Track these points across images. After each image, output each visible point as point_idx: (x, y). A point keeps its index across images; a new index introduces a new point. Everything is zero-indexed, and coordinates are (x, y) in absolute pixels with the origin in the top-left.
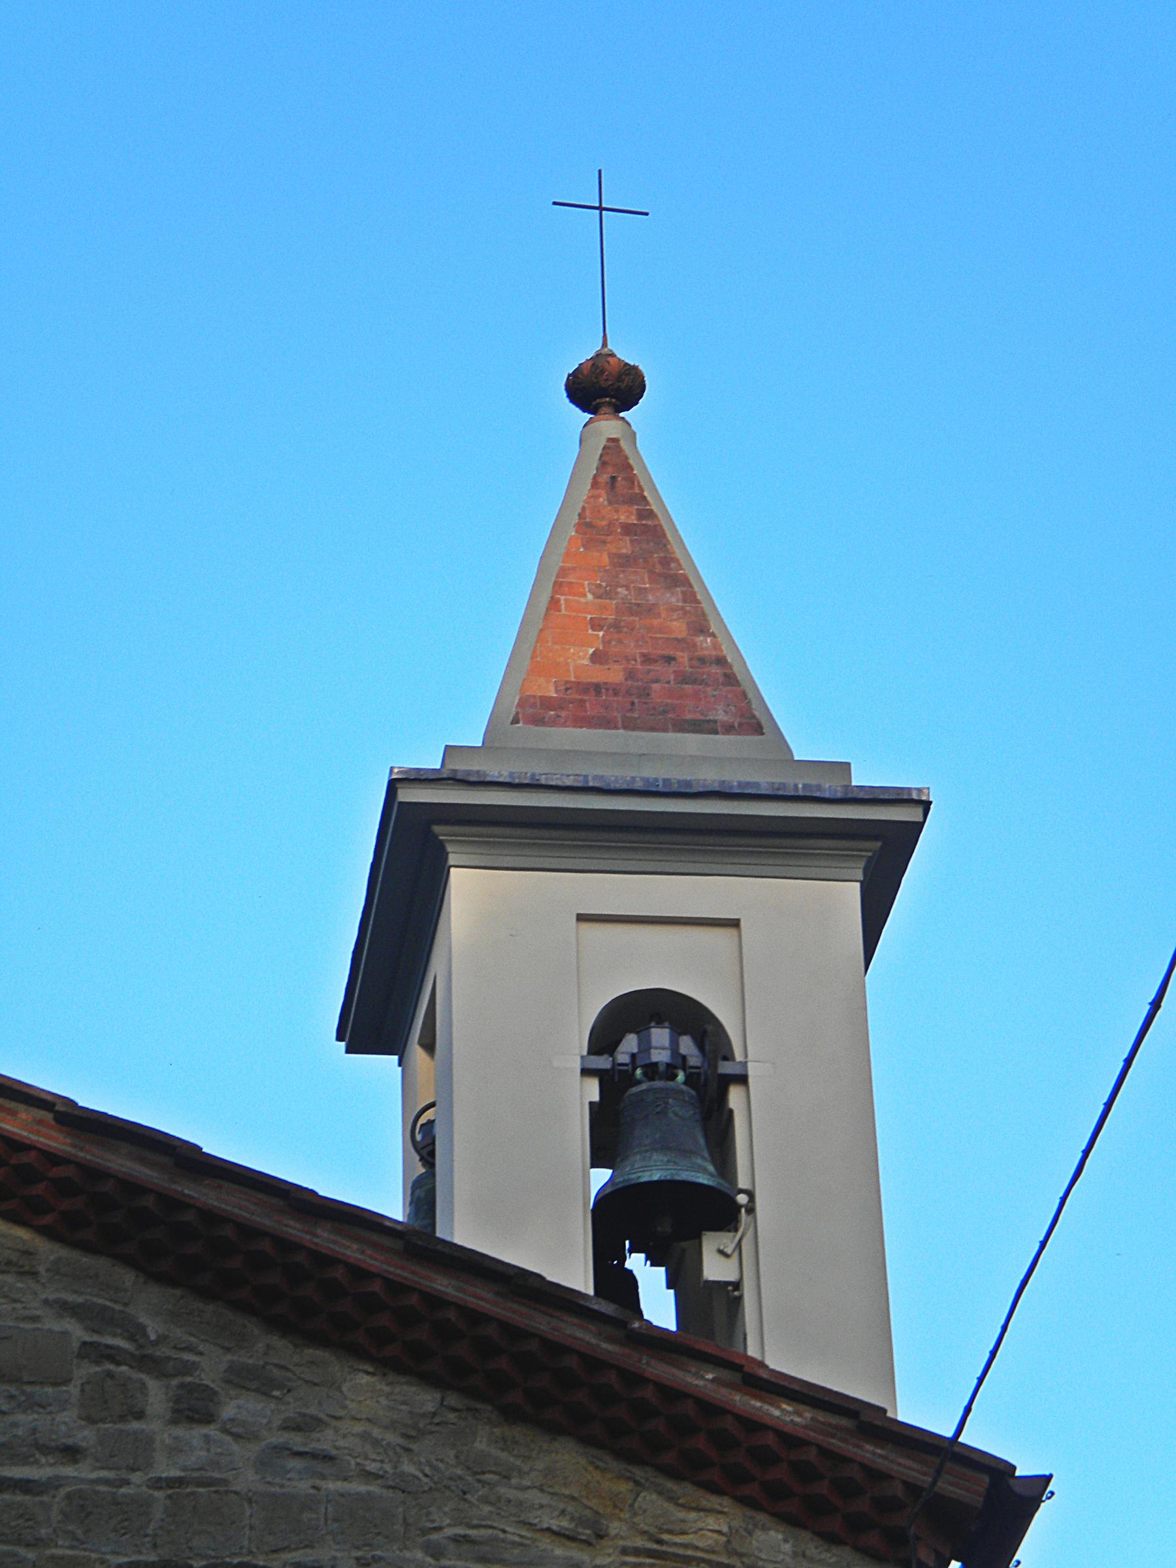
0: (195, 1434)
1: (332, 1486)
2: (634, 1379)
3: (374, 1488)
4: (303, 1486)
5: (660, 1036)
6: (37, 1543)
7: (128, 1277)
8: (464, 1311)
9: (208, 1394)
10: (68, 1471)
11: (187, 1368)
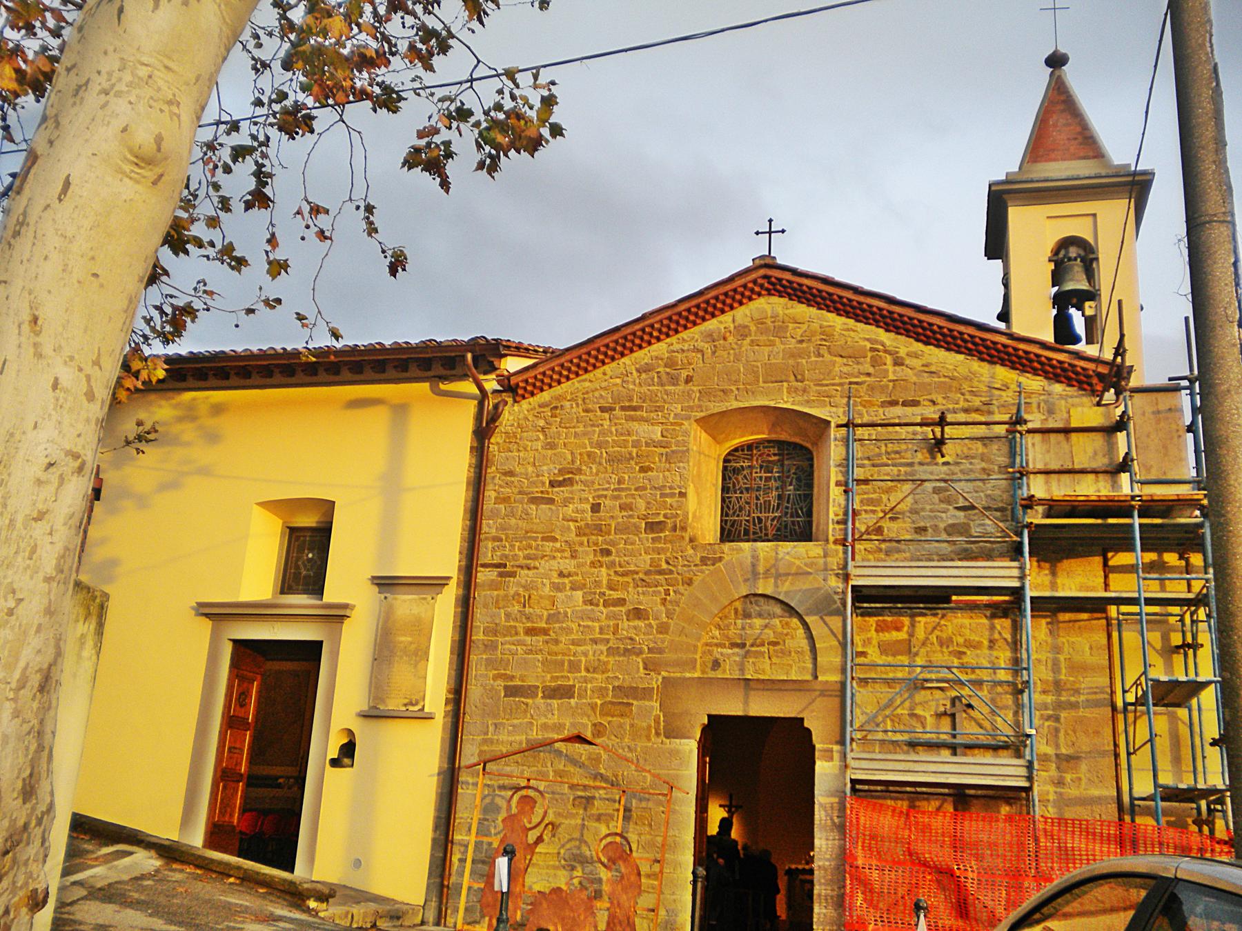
1: (937, 379)
2: (1016, 349)
4: (928, 380)
6: (860, 397)
9: (902, 358)
10: (868, 379)
11: (897, 352)
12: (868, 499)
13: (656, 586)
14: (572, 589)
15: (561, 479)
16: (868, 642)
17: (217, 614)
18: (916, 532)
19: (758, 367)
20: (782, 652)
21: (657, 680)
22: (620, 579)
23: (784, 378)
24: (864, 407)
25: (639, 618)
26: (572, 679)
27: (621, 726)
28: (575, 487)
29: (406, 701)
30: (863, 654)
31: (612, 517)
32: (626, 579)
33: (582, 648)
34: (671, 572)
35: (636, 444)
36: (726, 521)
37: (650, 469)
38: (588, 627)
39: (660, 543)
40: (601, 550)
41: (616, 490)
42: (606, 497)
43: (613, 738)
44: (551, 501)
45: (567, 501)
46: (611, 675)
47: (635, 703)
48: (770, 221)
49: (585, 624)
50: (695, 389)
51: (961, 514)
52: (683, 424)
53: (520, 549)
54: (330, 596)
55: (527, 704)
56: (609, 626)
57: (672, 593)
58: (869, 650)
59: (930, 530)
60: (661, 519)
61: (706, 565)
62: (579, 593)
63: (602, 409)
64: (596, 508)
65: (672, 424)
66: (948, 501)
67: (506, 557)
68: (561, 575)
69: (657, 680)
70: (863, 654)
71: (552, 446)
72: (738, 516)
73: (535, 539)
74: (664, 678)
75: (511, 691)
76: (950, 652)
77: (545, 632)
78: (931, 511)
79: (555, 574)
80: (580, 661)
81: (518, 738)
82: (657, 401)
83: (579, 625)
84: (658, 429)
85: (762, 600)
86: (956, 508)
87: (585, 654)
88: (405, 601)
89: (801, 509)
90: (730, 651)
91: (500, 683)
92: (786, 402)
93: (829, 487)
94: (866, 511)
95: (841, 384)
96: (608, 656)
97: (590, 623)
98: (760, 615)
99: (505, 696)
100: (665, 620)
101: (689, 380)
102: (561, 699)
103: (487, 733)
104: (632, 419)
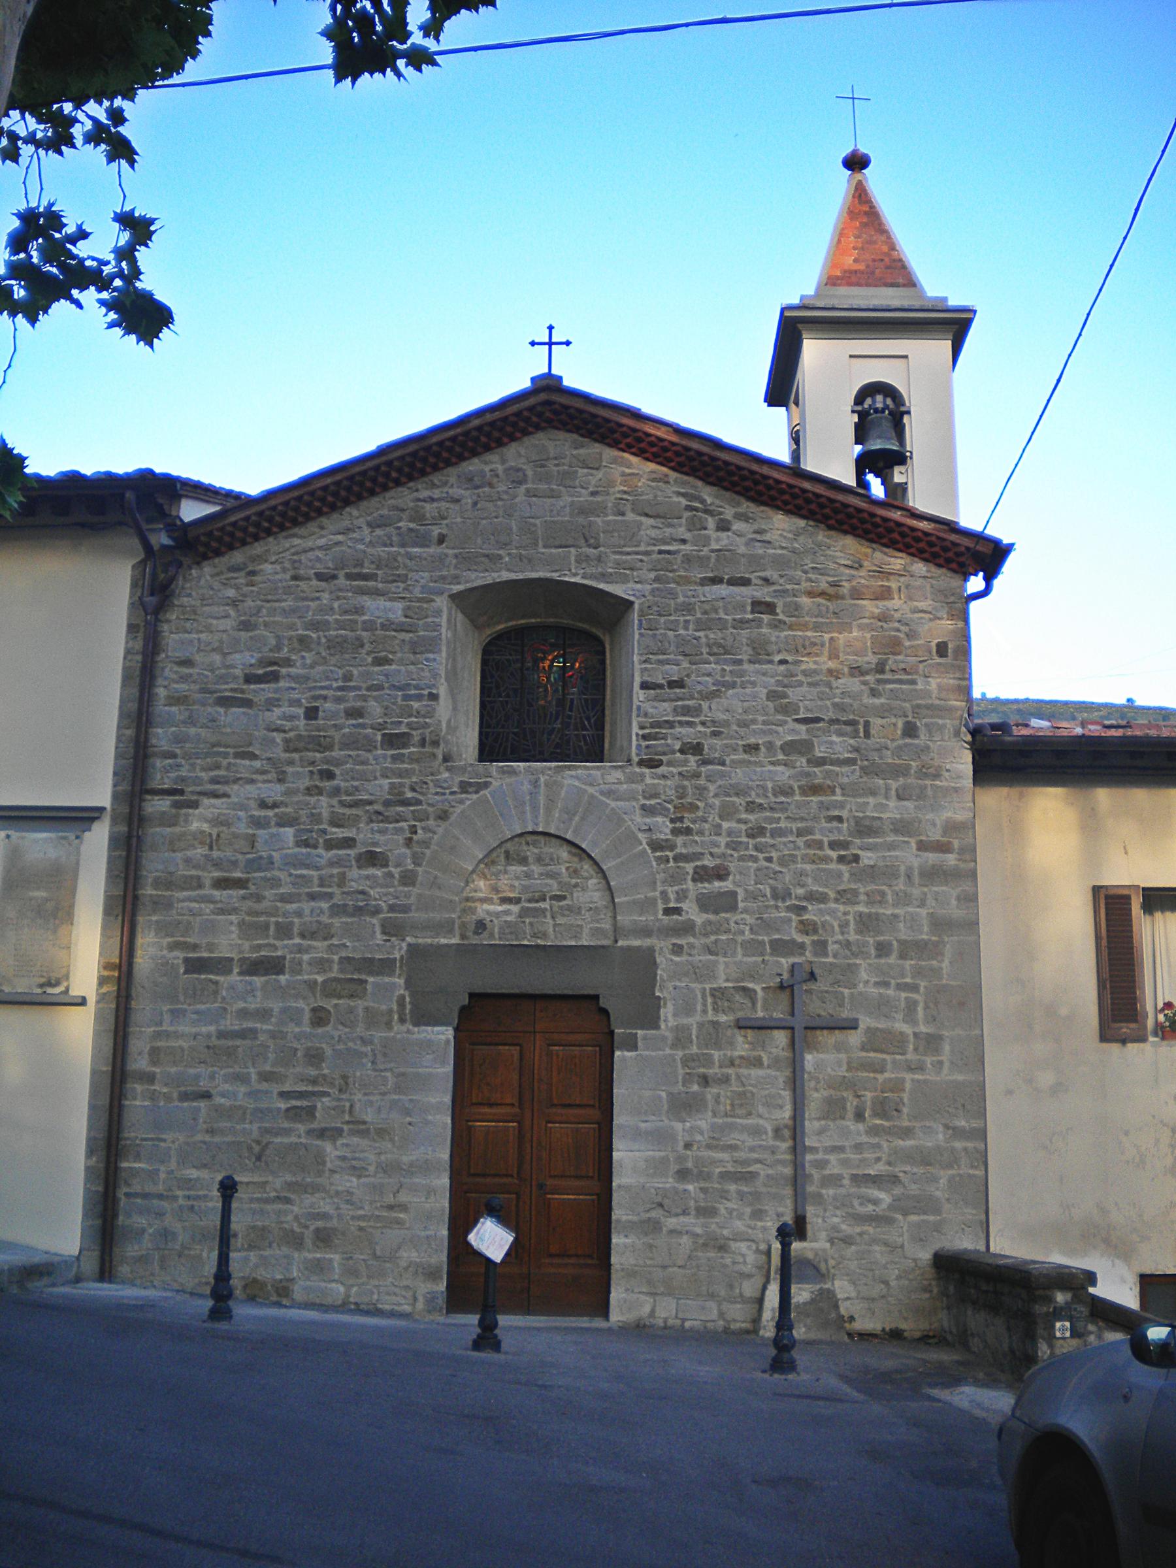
0: (724, 535)
2: (873, 515)
3: (784, 552)
4: (761, 551)
5: (879, 398)
7: (700, 483)
8: (814, 494)
9: (729, 522)
10: (683, 547)
11: (721, 513)
12: (683, 707)
13: (397, 821)
14: (279, 825)
15: (260, 672)
16: (682, 896)
18: (745, 751)
19: (535, 525)
20: (569, 908)
21: (400, 949)
22: (348, 811)
23: (570, 542)
24: (678, 583)
25: (374, 865)
26: (282, 948)
27: (351, 1011)
28: (282, 684)
29: (43, 980)
30: (677, 911)
31: (335, 726)
32: (354, 811)
33: (295, 906)
34: (419, 802)
35: (369, 626)
36: (487, 734)
37: (388, 661)
38: (302, 876)
39: (403, 762)
40: (321, 772)
41: (340, 689)
42: (325, 698)
43: (341, 1027)
44: (248, 703)
45: (271, 704)
46: (335, 941)
47: (371, 979)
48: (551, 328)
49: (299, 872)
50: (451, 552)
51: (803, 728)
52: (433, 600)
53: (203, 769)
55: (216, 983)
56: (332, 876)
57: (420, 831)
58: (684, 906)
59: (763, 749)
60: (404, 729)
61: (467, 792)
62: (289, 832)
63: (320, 577)
64: (312, 713)
65: (419, 600)
66: (785, 710)
67: (183, 779)
68: (263, 805)
69: (400, 949)
70: (677, 911)
71: (246, 626)
72: (503, 727)
73: (225, 755)
74: (409, 945)
76: (787, 907)
77: (240, 884)
78: (764, 723)
79: (253, 804)
80: (292, 923)
81: (204, 1029)
82: (397, 568)
83: (291, 875)
84: (399, 606)
85: (541, 839)
86: (796, 720)
87: (299, 914)
88: (35, 841)
89: (588, 719)
90: (500, 908)
91: (180, 955)
92: (575, 575)
93: (632, 691)
94: (680, 722)
95: (647, 553)
96: (331, 916)
97: (305, 872)
98: (539, 860)
99: (186, 972)
100: (411, 867)
101: (441, 540)
102: (266, 974)
103: (160, 1024)
104: (363, 592)
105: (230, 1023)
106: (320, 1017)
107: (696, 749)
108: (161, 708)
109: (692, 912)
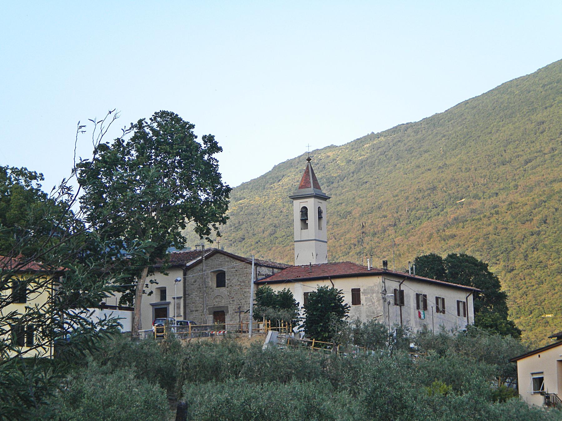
17: (153, 305)
26: (198, 309)
44: (193, 285)
54: (167, 300)
64: (199, 285)
75: (191, 311)
105: (194, 316)
106: (201, 315)
107: (231, 286)
108: (186, 286)
109: (231, 302)
